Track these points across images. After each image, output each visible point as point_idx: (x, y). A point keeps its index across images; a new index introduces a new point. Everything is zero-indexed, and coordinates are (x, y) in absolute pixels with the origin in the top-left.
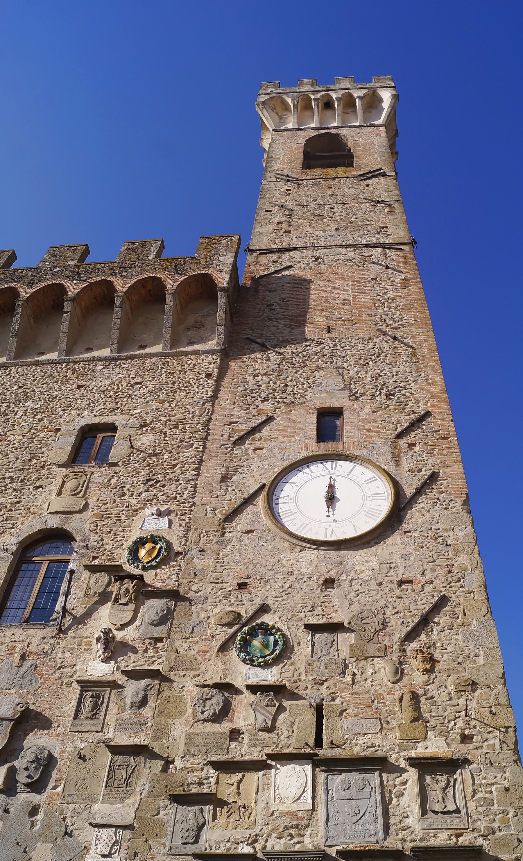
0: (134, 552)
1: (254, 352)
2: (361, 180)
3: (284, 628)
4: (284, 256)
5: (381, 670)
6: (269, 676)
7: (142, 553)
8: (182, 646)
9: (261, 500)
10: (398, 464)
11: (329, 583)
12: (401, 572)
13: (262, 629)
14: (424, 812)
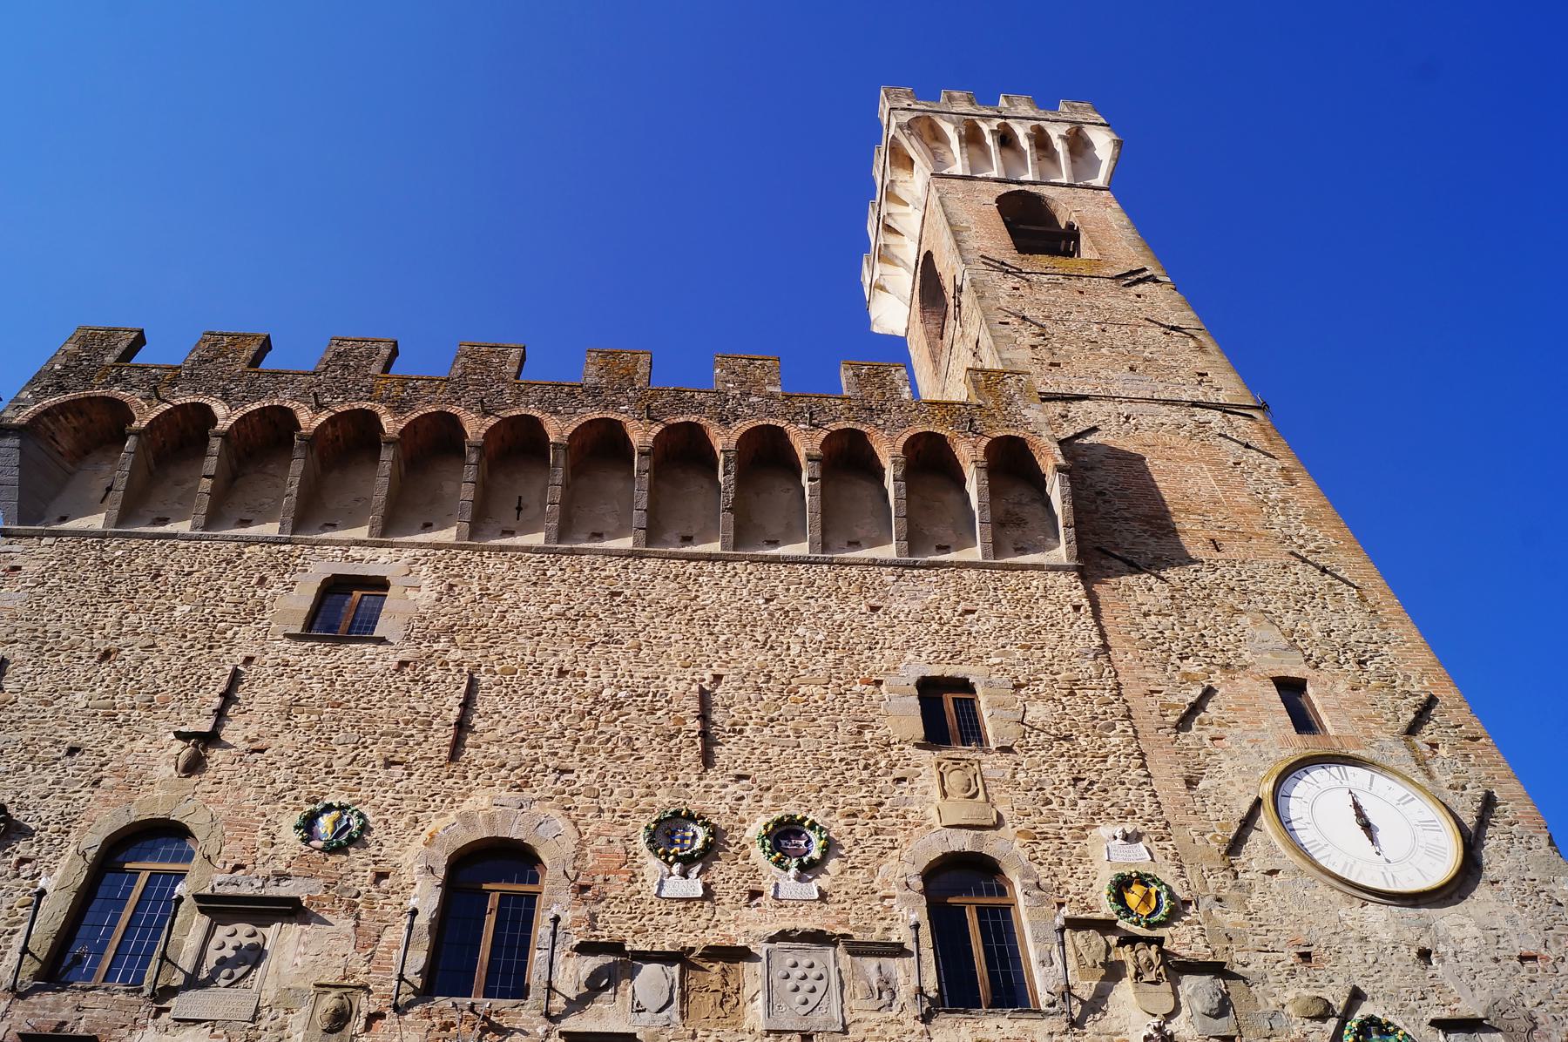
1: (1119, 574)
2: (1129, 285)
3: (1399, 1023)
4: (1074, 407)
7: (1133, 898)
9: (1265, 819)
11: (1425, 954)
12: (1516, 943)
13: (1372, 1024)
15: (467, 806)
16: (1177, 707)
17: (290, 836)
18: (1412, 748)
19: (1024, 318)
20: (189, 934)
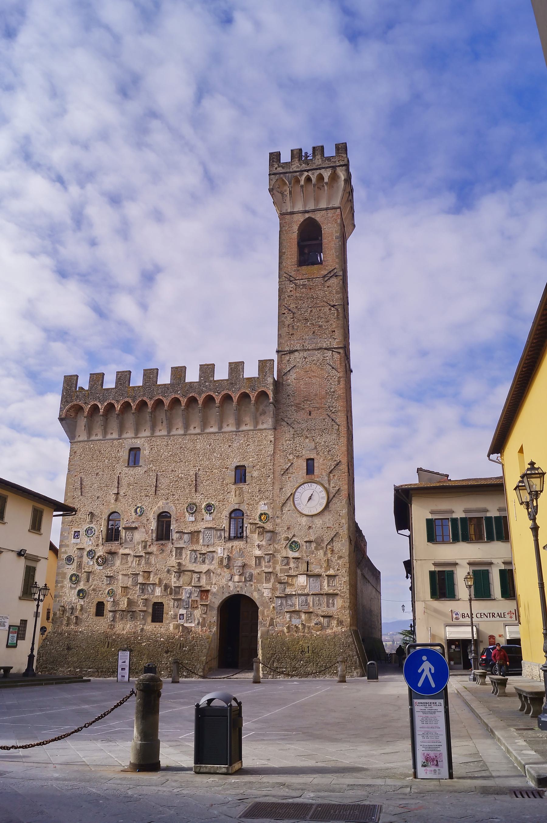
0: (260, 517)
4: (292, 356)
5: (321, 553)
6: (296, 555)
8: (276, 546)
10: (329, 485)
14: (328, 586)
17: (134, 514)
18: (329, 477)
20: (123, 533)
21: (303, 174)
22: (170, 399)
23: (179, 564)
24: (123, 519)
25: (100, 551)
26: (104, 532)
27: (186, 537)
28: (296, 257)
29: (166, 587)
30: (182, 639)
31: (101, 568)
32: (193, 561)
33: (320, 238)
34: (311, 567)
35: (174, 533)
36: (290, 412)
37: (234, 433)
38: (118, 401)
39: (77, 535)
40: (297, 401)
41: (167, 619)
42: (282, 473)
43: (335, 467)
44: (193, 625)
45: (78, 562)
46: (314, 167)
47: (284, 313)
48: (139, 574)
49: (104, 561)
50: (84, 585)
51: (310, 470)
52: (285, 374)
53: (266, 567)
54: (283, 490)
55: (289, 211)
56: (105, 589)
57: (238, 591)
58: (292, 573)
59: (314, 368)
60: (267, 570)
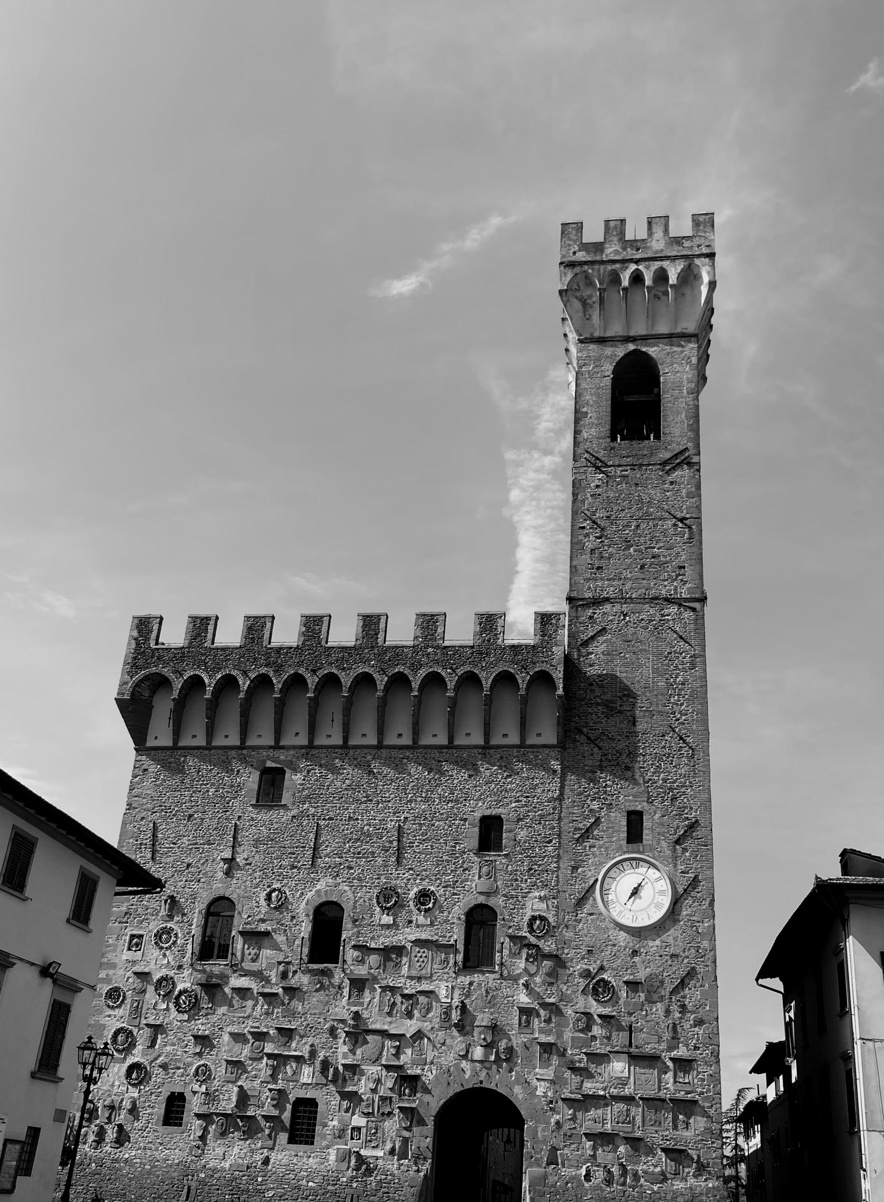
5: (660, 1007)
11: (635, 953)
14: (675, 1082)
15: (318, 887)
16: (581, 829)
17: (263, 903)
18: (675, 850)
19: (594, 522)
20: (239, 943)
21: (627, 268)
22: (353, 674)
23: (357, 1016)
24: (239, 913)
25: (185, 982)
26: (198, 939)
27: (374, 959)
28: (609, 423)
29: (325, 1065)
30: (355, 1185)
31: (186, 1017)
32: (387, 1009)
33: (656, 390)
34: (639, 1038)
35: (348, 947)
36: (594, 717)
37: (480, 750)
38: (245, 673)
39: (136, 942)
40: (608, 697)
41: (324, 1137)
42: (577, 836)
43: (686, 832)
44: (380, 1153)
45: (133, 1002)
46: (649, 255)
47: (583, 528)
48: (268, 1033)
49: (191, 1007)
50: (144, 1054)
51: (634, 834)
52: (585, 644)
53: (541, 1031)
54: (580, 870)
55: (597, 334)
56: (190, 1064)
57: (481, 1082)
58: (598, 1047)
59: (643, 634)
60: (544, 1039)
